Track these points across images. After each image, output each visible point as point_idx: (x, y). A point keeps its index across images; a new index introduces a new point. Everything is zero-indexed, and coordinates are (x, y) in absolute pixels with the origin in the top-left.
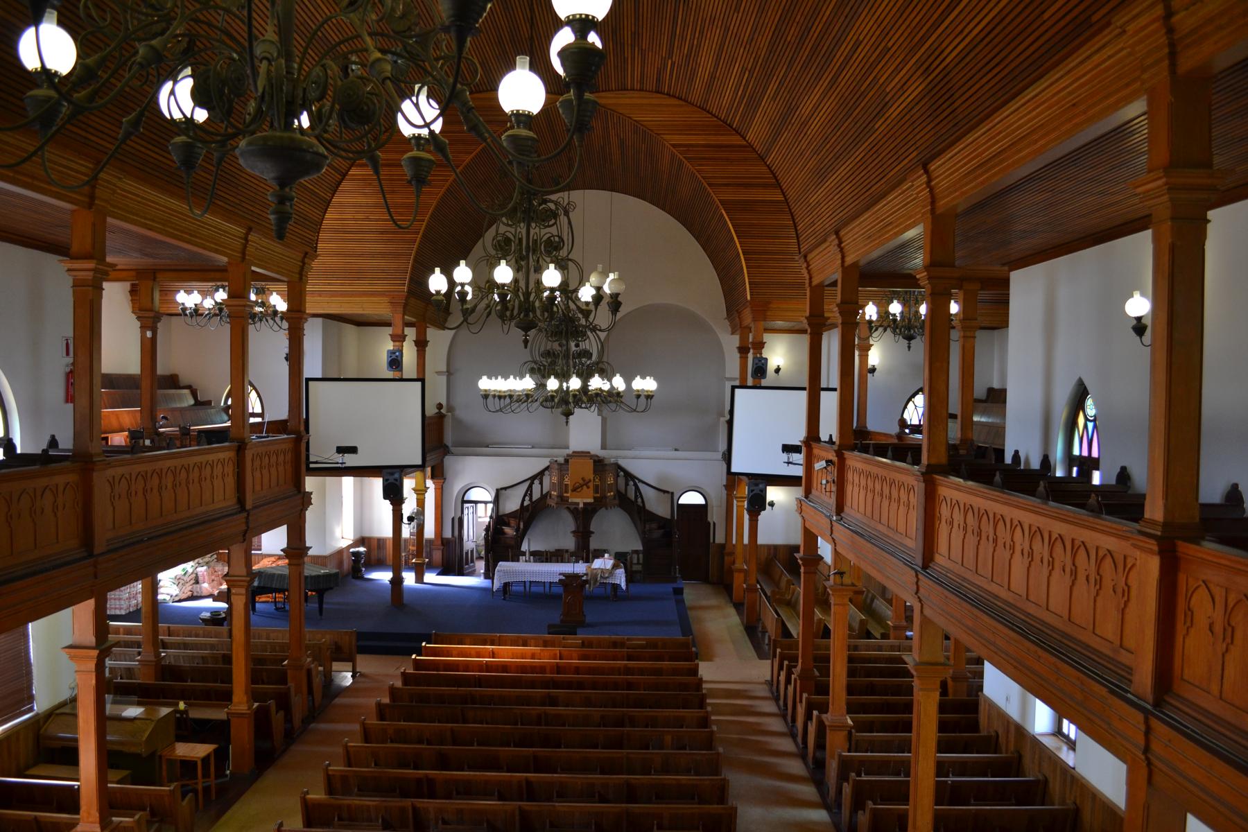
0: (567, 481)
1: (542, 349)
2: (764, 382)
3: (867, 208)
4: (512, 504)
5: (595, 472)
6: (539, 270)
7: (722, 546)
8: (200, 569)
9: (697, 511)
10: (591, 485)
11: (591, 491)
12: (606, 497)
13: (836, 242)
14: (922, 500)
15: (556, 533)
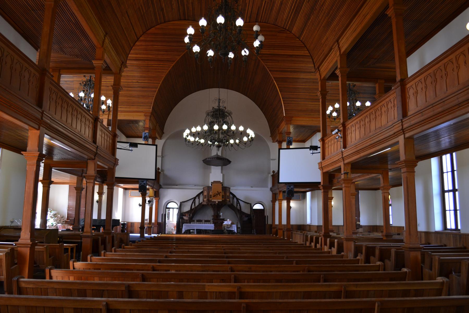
0: (211, 193)
3: (355, 16)
4: (187, 208)
7: (271, 225)
10: (221, 194)
11: (221, 197)
13: (337, 46)
14: (400, 94)
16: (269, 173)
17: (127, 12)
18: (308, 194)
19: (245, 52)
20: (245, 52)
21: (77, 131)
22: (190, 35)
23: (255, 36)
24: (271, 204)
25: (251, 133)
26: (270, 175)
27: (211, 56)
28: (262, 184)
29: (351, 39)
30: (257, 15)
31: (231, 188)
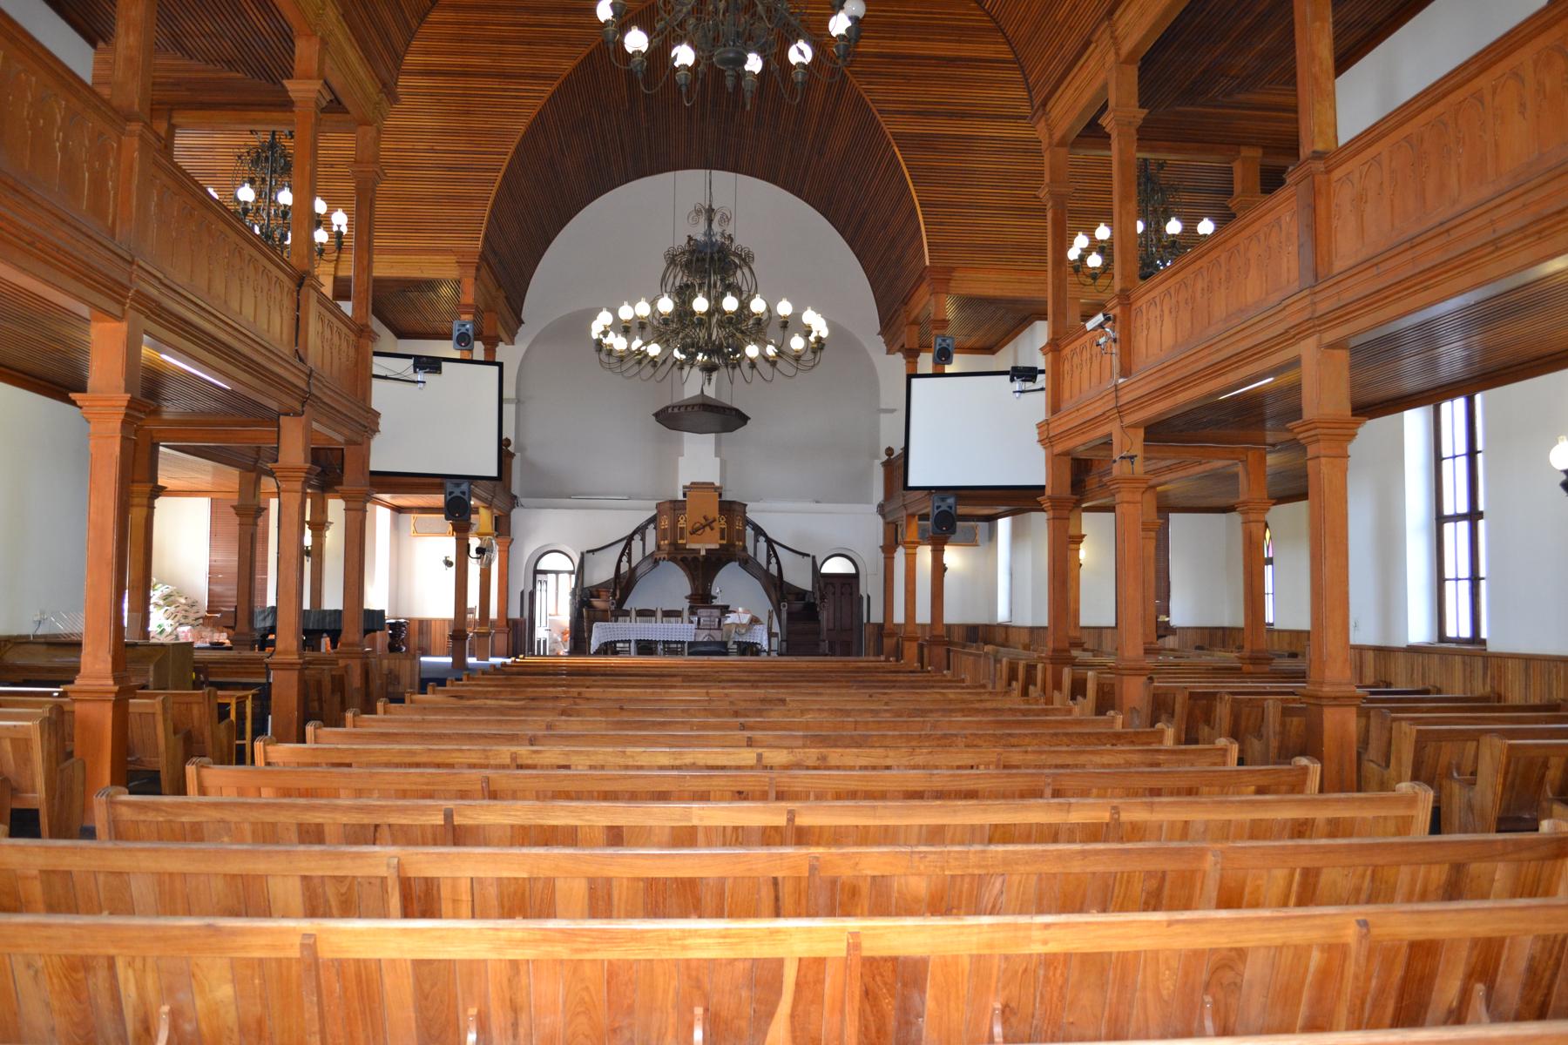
0: (682, 524)
2: (948, 369)
4: (602, 571)
7: (880, 627)
8: (181, 629)
9: (848, 583)
12: (734, 545)
15: (674, 587)
16: (877, 457)
18: (1004, 525)
19: (801, 52)
21: (244, 323)
25: (817, 323)
28: (852, 492)
31: (750, 506)
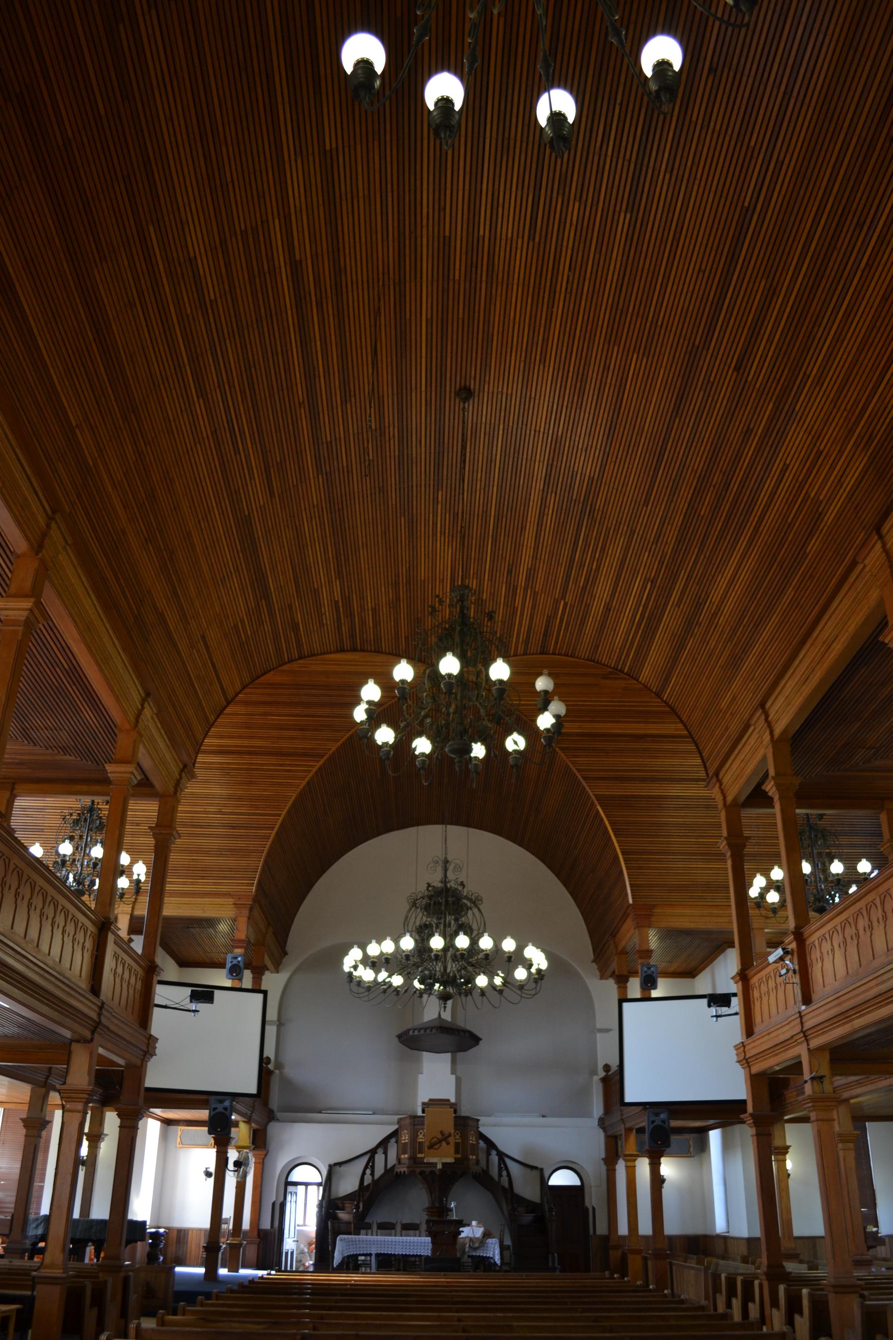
0: (421, 1138)
1: (418, 924)
3: (803, 642)
4: (348, 1185)
5: (456, 1125)
6: (488, 662)
7: (606, 1239)
10: (451, 1140)
12: (468, 1159)
13: (763, 717)
16: (594, 1072)
17: (203, 637)
18: (715, 1137)
19: (516, 743)
20: (515, 742)
21: (50, 962)
22: (369, 703)
23: (539, 701)
24: (604, 1168)
25: (537, 958)
26: (596, 1079)
27: (423, 754)
28: (574, 1107)
29: (798, 701)
30: (545, 635)
31: (483, 1120)
